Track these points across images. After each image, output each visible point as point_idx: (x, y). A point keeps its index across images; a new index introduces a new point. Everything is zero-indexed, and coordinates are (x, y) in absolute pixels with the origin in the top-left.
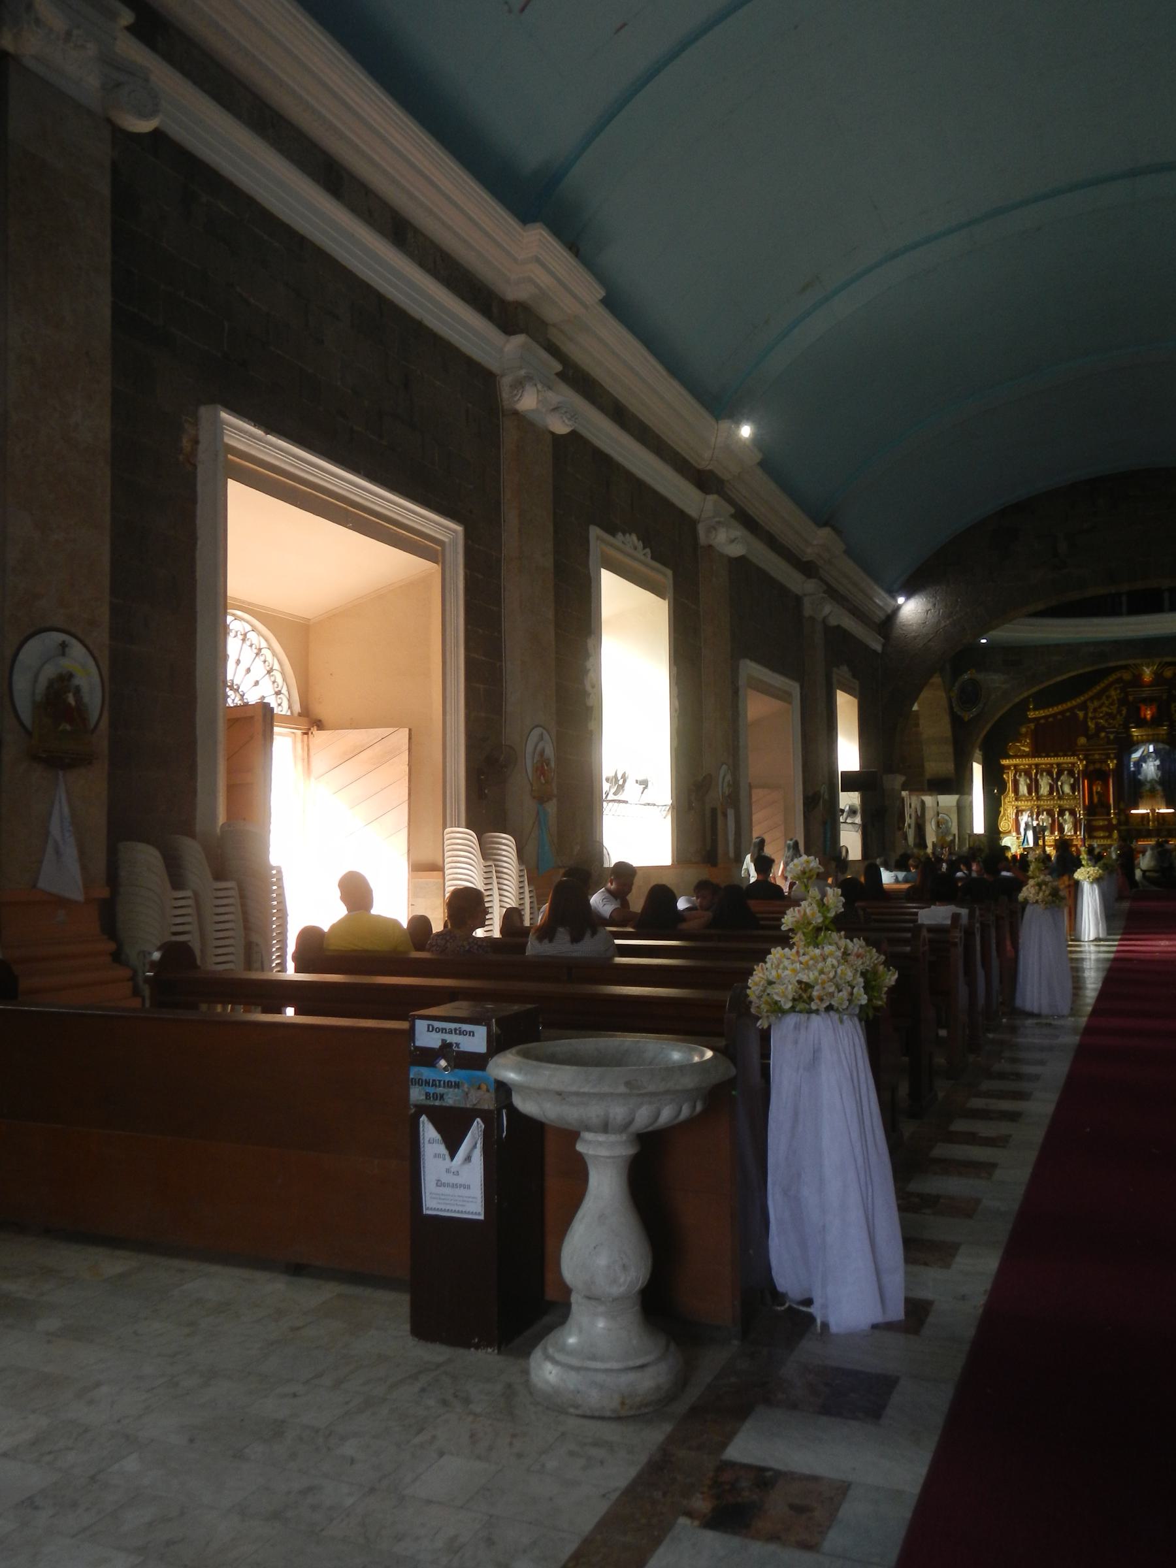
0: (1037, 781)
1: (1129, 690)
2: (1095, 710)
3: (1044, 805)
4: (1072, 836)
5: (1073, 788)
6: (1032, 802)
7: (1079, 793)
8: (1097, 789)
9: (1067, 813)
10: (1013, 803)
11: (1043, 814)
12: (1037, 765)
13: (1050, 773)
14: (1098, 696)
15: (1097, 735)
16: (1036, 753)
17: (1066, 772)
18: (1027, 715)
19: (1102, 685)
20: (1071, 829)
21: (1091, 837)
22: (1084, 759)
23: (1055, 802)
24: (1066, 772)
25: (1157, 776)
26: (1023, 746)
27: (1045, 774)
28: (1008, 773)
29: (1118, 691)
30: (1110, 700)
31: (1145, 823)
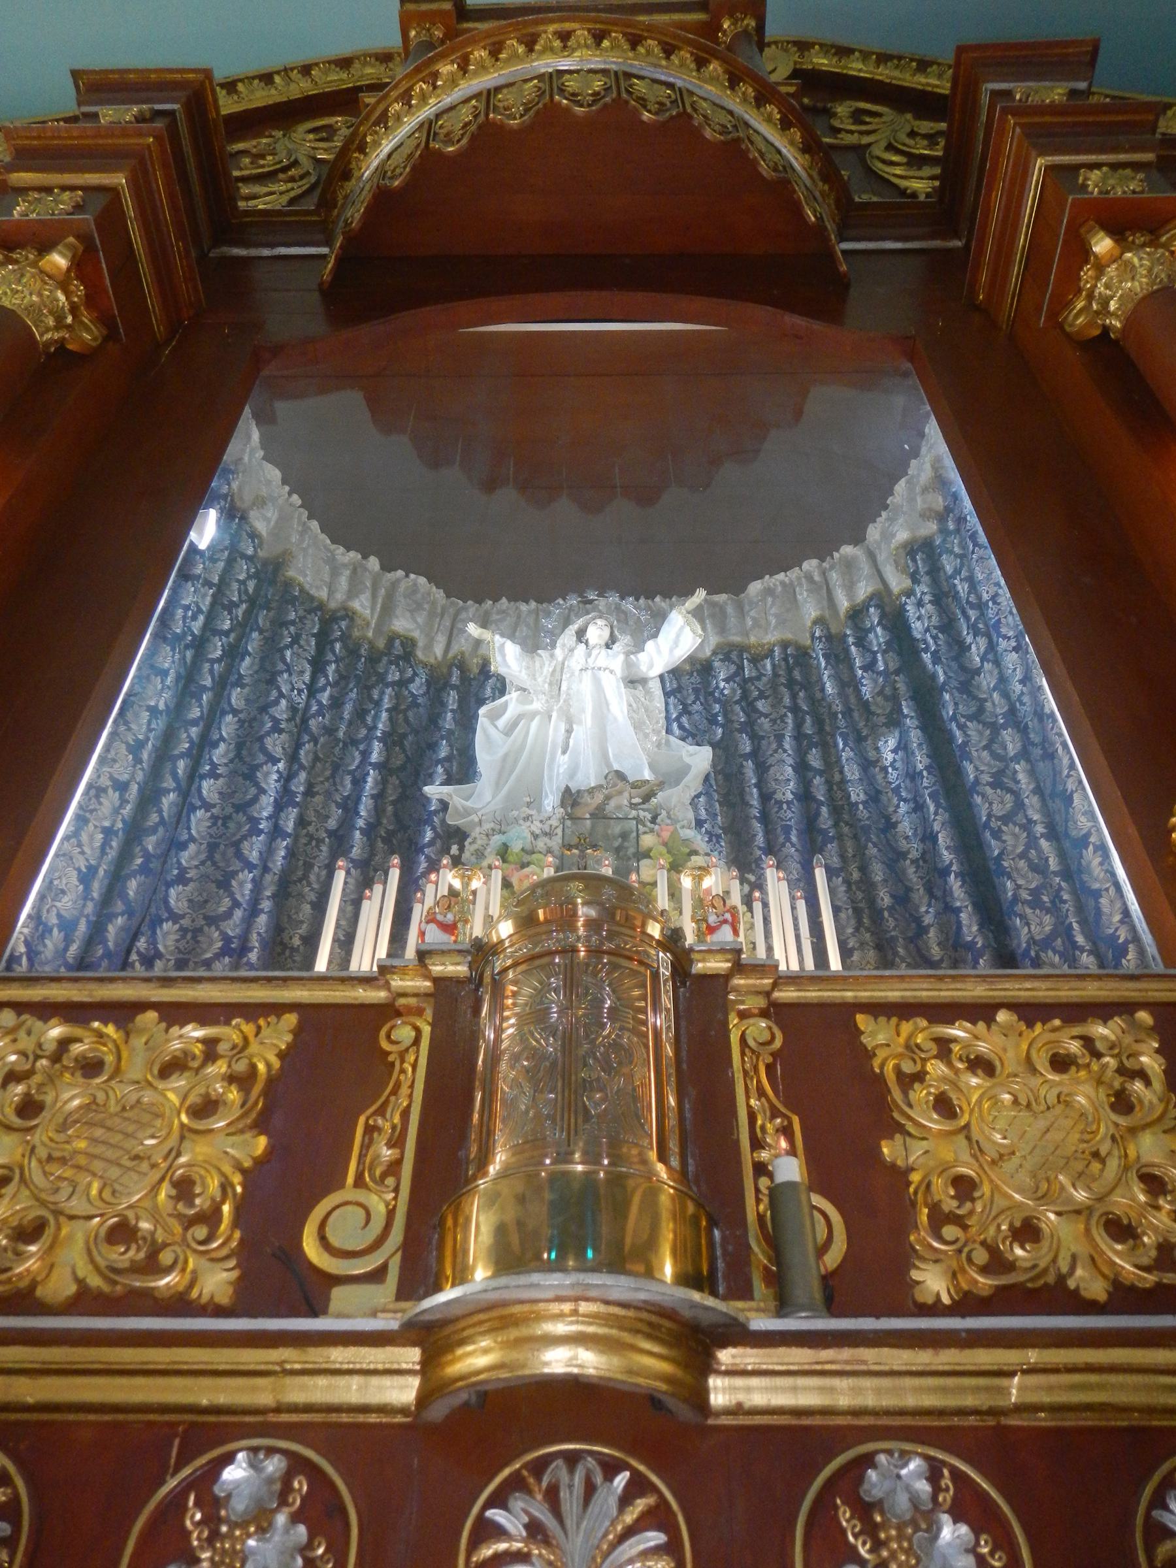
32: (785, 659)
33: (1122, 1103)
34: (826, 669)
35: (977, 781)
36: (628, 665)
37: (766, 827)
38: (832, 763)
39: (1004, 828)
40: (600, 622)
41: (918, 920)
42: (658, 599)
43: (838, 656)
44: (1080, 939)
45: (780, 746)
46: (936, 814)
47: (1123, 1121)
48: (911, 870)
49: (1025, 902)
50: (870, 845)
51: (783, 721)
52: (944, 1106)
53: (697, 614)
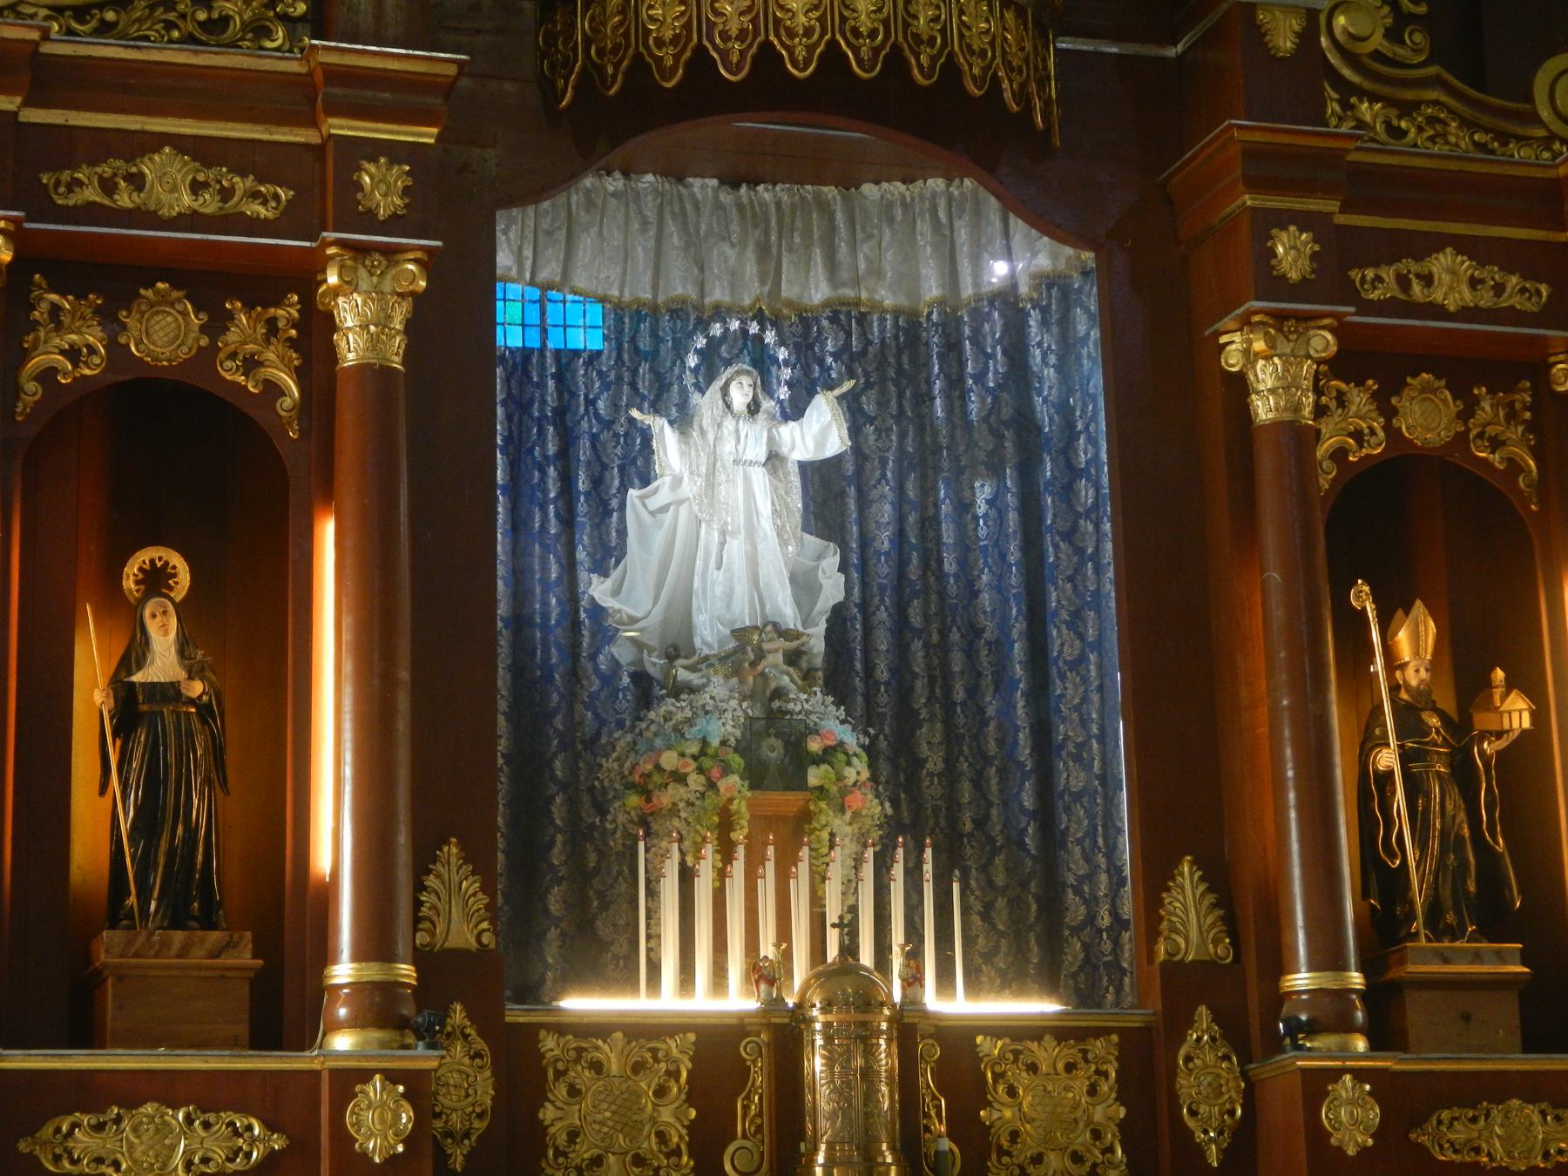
8: (136, 652)
25: (805, 586)
32: (896, 337)
33: (1092, 1091)
34: (938, 377)
35: (1056, 613)
36: (771, 440)
37: (863, 576)
38: (927, 491)
39: (1068, 674)
40: (746, 381)
41: (981, 711)
42: (761, 188)
43: (952, 347)
44: (1100, 841)
45: (884, 475)
46: (1016, 619)
47: (1089, 1100)
48: (984, 652)
49: (1070, 754)
50: (955, 629)
51: (888, 436)
52: (1012, 1092)
53: (840, 399)
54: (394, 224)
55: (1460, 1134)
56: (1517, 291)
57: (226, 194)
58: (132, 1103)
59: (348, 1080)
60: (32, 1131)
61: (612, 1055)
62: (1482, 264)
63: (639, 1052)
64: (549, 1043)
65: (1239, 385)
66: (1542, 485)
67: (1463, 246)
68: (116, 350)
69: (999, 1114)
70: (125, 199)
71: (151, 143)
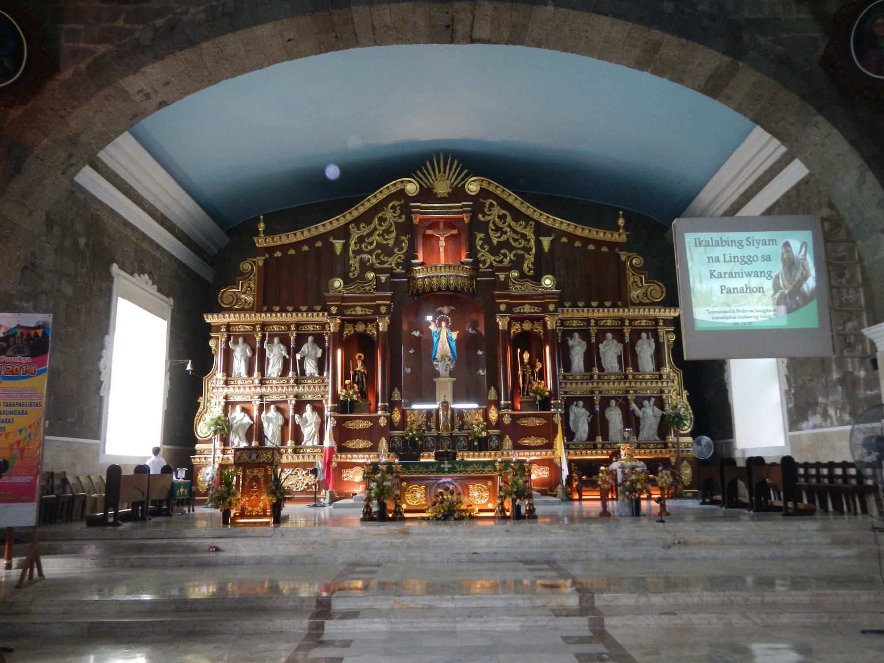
0: (262, 352)
1: (411, 204)
2: (361, 240)
3: (272, 394)
4: (314, 447)
5: (321, 365)
6: (253, 389)
7: (328, 374)
9: (308, 407)
10: (221, 390)
11: (267, 411)
12: (264, 326)
13: (285, 340)
14: (366, 218)
15: (362, 277)
16: (264, 303)
17: (310, 339)
18: (254, 244)
19: (374, 201)
20: (314, 435)
21: (342, 449)
22: (336, 315)
23: (290, 389)
24: (310, 339)
26: (245, 293)
27: (276, 340)
28: (217, 338)
29: (398, 211)
30: (385, 225)
31: (433, 425)
54: (385, 314)
55: (523, 422)
56: (536, 309)
57: (365, 311)
58: (355, 420)
59: (379, 417)
60: (344, 423)
61: (416, 412)
62: (532, 306)
63: (419, 412)
64: (408, 412)
65: (498, 324)
66: (543, 334)
67: (529, 304)
68: (355, 331)
69: (466, 419)
70: (353, 313)
71: (356, 306)
